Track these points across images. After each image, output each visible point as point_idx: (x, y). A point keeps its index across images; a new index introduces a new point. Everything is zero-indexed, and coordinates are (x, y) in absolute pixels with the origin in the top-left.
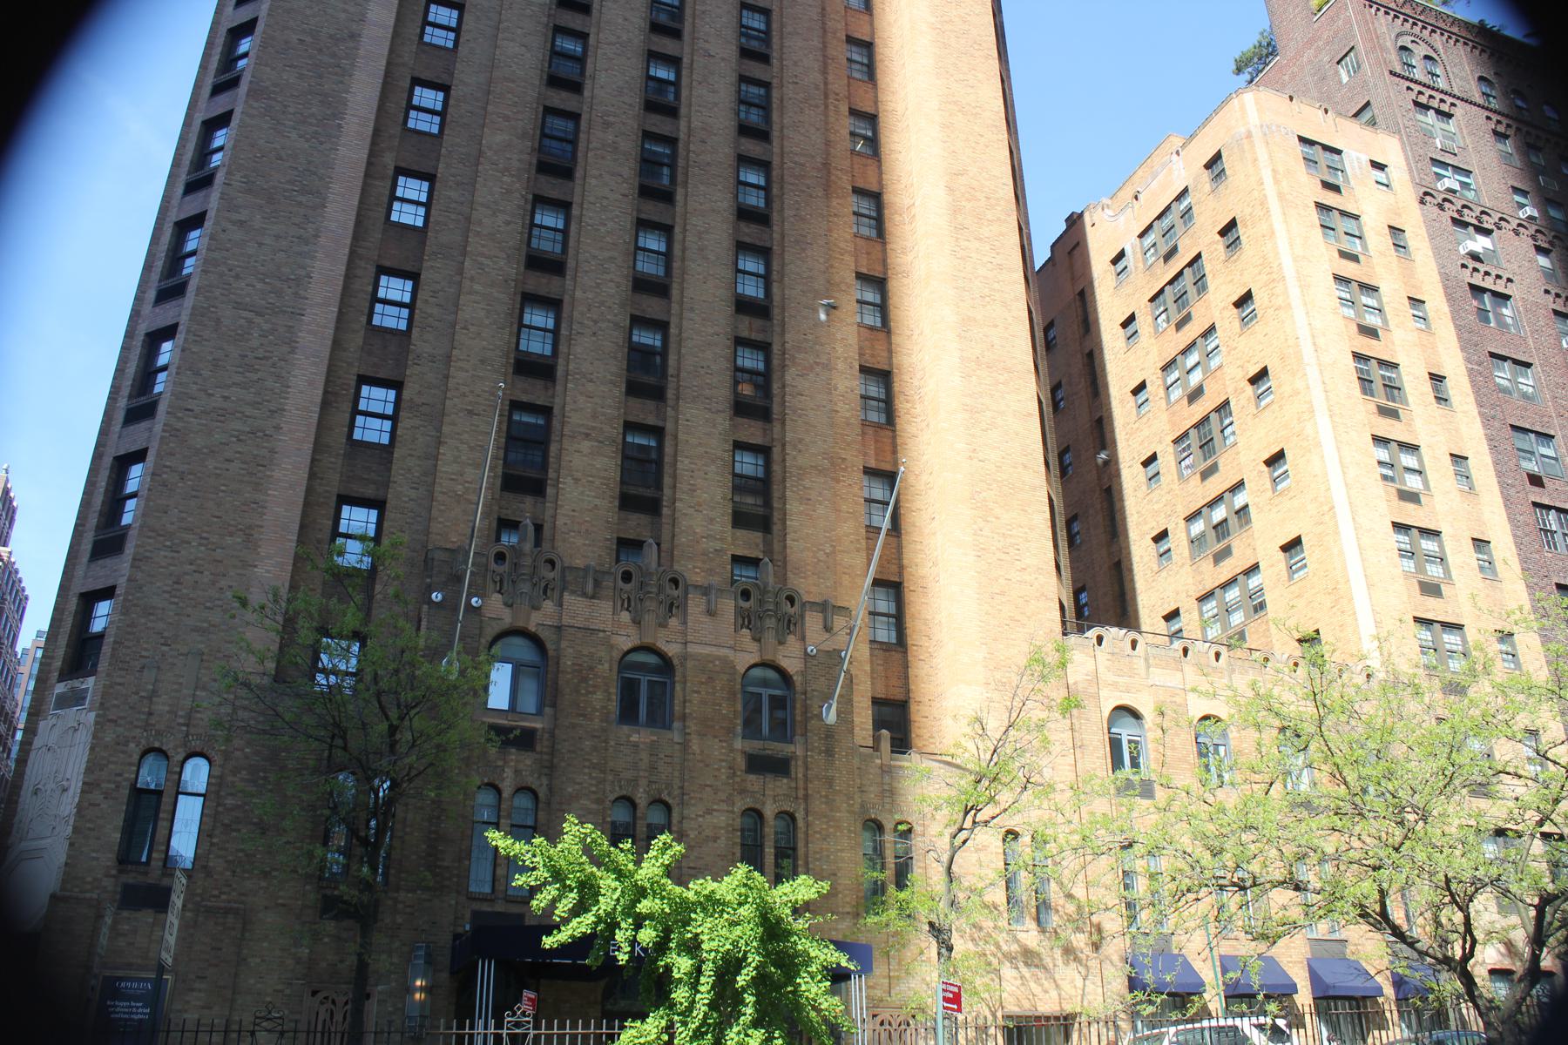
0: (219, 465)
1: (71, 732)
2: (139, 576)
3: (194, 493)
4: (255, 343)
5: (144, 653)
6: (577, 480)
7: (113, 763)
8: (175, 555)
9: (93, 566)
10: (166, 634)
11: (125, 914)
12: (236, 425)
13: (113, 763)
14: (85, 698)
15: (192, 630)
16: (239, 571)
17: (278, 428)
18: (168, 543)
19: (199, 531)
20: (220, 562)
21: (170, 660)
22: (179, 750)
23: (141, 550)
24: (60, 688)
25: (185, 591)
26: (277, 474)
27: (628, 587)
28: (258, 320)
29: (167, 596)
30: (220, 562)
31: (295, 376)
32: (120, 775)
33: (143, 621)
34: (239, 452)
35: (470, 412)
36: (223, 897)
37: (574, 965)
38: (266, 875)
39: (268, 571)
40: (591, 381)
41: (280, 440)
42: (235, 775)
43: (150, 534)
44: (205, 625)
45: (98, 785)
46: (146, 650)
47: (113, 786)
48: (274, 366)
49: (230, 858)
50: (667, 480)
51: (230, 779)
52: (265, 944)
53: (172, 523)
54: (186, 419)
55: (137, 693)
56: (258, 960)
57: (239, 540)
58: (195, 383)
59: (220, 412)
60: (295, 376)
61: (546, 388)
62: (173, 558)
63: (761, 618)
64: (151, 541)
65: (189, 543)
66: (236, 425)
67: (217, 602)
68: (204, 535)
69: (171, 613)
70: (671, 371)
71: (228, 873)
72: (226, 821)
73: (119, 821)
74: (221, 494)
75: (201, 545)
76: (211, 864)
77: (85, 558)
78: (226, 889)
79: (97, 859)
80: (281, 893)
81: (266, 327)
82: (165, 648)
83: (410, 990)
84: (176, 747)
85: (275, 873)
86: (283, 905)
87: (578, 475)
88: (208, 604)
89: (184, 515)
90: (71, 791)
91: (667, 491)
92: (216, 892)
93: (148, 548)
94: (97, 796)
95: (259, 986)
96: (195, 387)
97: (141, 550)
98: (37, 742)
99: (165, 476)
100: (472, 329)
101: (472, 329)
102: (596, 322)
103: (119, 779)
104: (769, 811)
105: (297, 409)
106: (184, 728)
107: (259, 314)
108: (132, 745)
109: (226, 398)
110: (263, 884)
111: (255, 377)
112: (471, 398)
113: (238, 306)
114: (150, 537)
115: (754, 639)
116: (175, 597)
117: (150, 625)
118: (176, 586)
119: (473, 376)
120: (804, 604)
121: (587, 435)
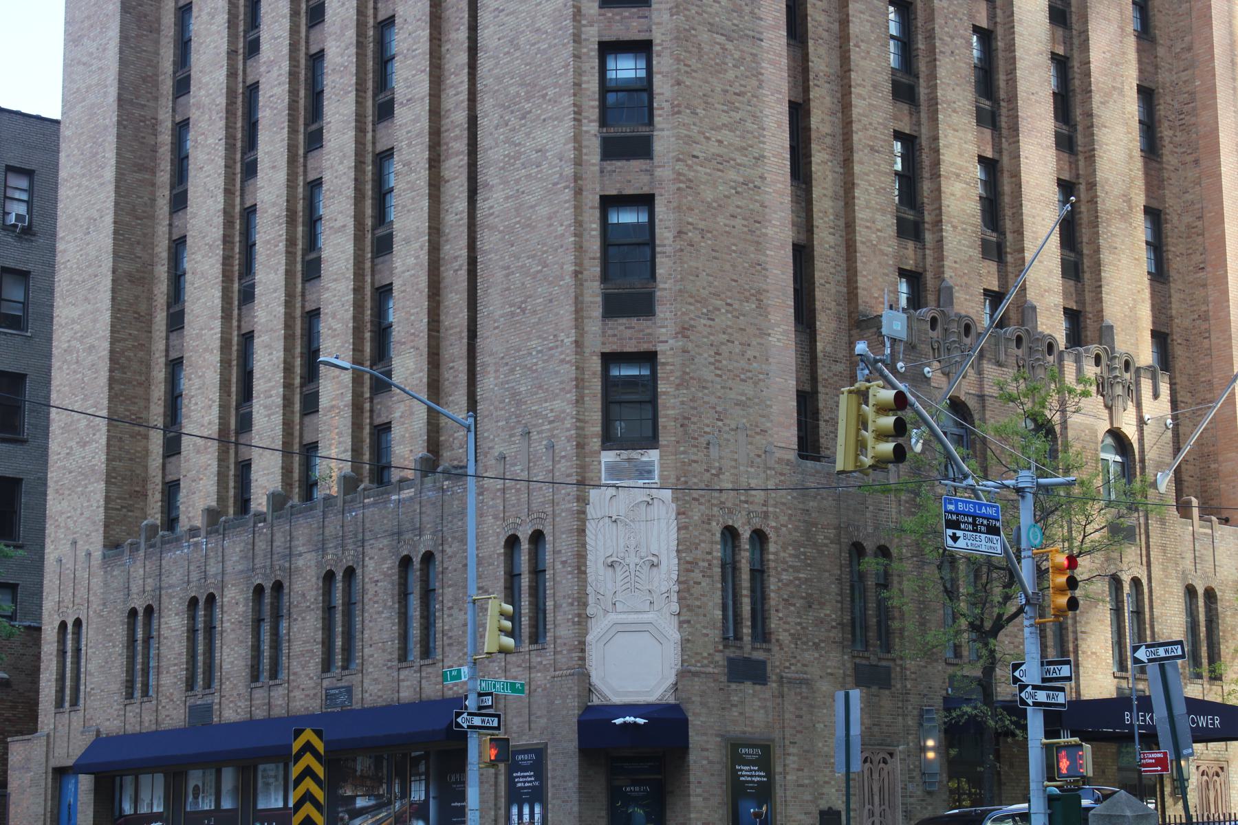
0: (727, 222)
1: (643, 506)
2: (690, 346)
3: (714, 254)
4: (731, 75)
5: (707, 429)
6: (955, 227)
7: (704, 541)
8: (711, 323)
9: (610, 323)
10: (718, 409)
11: (733, 686)
12: (732, 175)
13: (704, 541)
14: (650, 472)
15: (736, 404)
16: (759, 340)
17: (762, 178)
18: (705, 311)
19: (723, 296)
20: (745, 330)
21: (725, 436)
22: (746, 527)
23: (686, 318)
24: (608, 457)
25: (724, 362)
26: (770, 231)
27: (1020, 352)
28: (729, 46)
29: (712, 367)
30: (745, 330)
31: (767, 116)
32: (709, 553)
33: (700, 395)
34: (738, 207)
35: (872, 149)
36: (793, 668)
37: (1114, 732)
38: (816, 646)
39: (779, 340)
40: (955, 111)
41: (767, 193)
42: (785, 551)
43: (692, 300)
44: (744, 398)
45: (697, 564)
46: (708, 426)
47: (706, 564)
48: (749, 103)
49: (792, 631)
50: (1008, 224)
51: (782, 554)
52: (825, 711)
53: (704, 288)
54: (695, 167)
55: (708, 471)
56: (822, 725)
57: (754, 306)
58: (694, 124)
59: (719, 159)
60: (767, 116)
61: (911, 114)
62: (710, 326)
63: (1112, 385)
64: (692, 308)
65: (719, 310)
66: (732, 175)
67: (749, 374)
68: (729, 301)
69: (719, 387)
70: (1002, 95)
71: (793, 646)
72: (785, 596)
73: (717, 597)
74: (734, 255)
75: (727, 311)
76: (781, 638)
77: (597, 312)
78: (793, 661)
79: (707, 635)
80: (829, 663)
81: (737, 55)
82: (720, 423)
83: (924, 749)
84: (744, 524)
85: (823, 645)
86: (831, 674)
87: (955, 221)
88: (743, 376)
89: (711, 279)
90: (664, 567)
91: (1010, 237)
92: (787, 664)
93: (692, 316)
94: (697, 575)
95: (826, 749)
96: (695, 129)
97: (686, 318)
98: (591, 511)
99: (690, 234)
100: (863, 46)
101: (863, 46)
102: (952, 38)
103: (709, 557)
104: (1126, 578)
105: (774, 156)
106: (746, 506)
107: (730, 39)
108: (714, 524)
109: (720, 142)
110: (816, 655)
111: (737, 116)
112: (871, 132)
113: (712, 28)
114: (690, 304)
115: (1106, 406)
116: (717, 368)
117: (706, 399)
118: (718, 357)
119: (870, 104)
120: (1138, 369)
121: (958, 176)
